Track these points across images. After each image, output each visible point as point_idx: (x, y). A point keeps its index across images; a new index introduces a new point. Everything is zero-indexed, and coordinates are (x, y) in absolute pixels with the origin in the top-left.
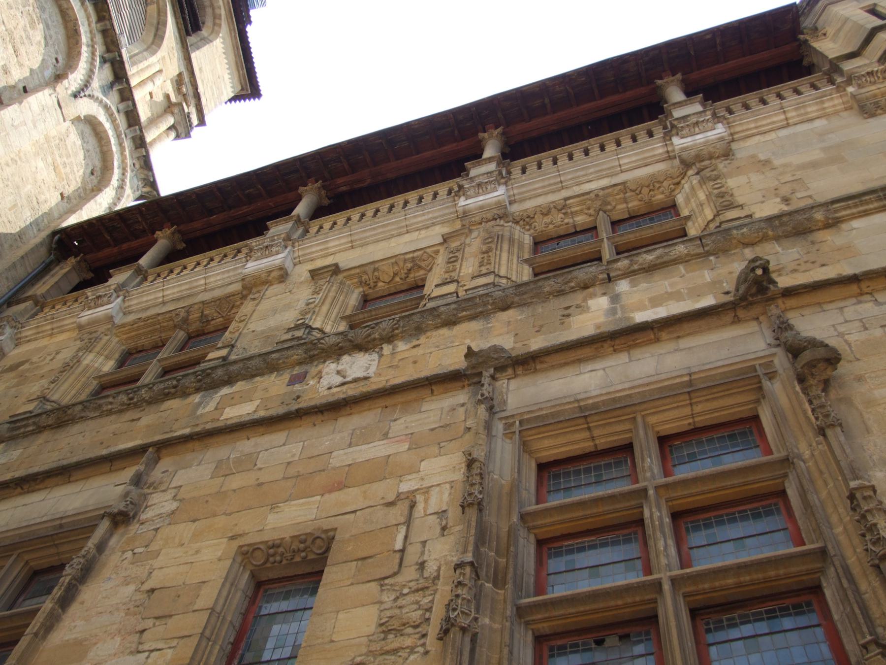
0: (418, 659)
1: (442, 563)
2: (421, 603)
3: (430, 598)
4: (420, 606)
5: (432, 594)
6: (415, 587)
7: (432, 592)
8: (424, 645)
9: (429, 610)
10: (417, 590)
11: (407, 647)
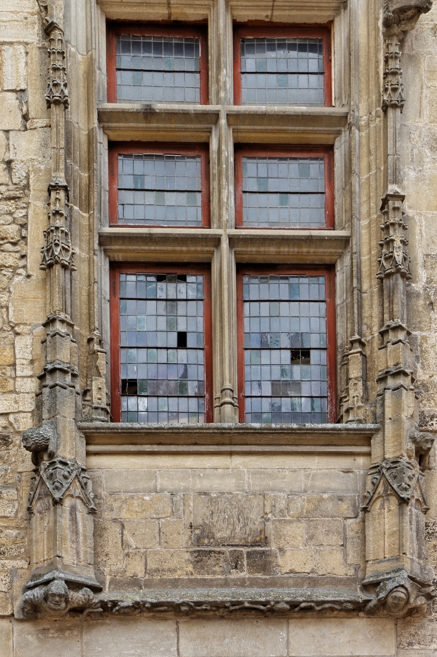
0: (23, 282)
1: (31, 169)
2: (15, 215)
3: (24, 212)
4: (14, 218)
5: (24, 208)
6: (7, 194)
7: (25, 205)
8: (25, 267)
9: (24, 226)
10: (9, 199)
11: (10, 266)
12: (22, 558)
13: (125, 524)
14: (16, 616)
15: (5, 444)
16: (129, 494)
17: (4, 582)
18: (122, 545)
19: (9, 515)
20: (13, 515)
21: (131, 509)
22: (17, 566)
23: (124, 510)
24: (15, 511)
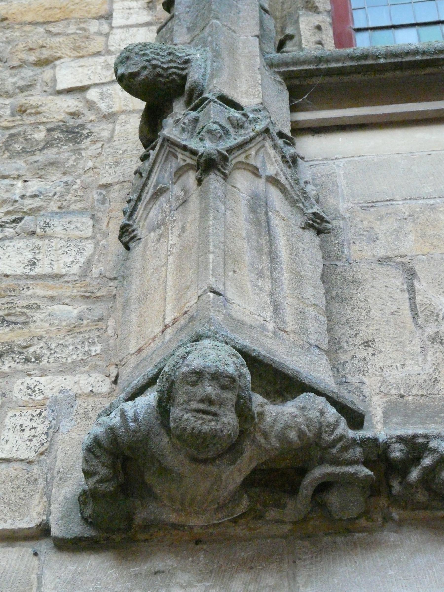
12: (95, 367)
13: (417, 268)
14: (55, 531)
15: (70, 140)
16: (420, 201)
17: (27, 433)
18: (415, 317)
19: (63, 271)
20: (75, 269)
21: (429, 232)
22: (76, 390)
23: (412, 237)
24: (82, 260)
